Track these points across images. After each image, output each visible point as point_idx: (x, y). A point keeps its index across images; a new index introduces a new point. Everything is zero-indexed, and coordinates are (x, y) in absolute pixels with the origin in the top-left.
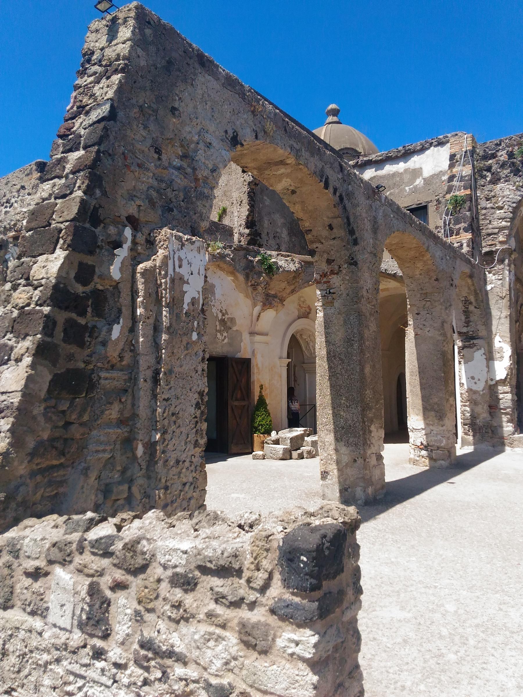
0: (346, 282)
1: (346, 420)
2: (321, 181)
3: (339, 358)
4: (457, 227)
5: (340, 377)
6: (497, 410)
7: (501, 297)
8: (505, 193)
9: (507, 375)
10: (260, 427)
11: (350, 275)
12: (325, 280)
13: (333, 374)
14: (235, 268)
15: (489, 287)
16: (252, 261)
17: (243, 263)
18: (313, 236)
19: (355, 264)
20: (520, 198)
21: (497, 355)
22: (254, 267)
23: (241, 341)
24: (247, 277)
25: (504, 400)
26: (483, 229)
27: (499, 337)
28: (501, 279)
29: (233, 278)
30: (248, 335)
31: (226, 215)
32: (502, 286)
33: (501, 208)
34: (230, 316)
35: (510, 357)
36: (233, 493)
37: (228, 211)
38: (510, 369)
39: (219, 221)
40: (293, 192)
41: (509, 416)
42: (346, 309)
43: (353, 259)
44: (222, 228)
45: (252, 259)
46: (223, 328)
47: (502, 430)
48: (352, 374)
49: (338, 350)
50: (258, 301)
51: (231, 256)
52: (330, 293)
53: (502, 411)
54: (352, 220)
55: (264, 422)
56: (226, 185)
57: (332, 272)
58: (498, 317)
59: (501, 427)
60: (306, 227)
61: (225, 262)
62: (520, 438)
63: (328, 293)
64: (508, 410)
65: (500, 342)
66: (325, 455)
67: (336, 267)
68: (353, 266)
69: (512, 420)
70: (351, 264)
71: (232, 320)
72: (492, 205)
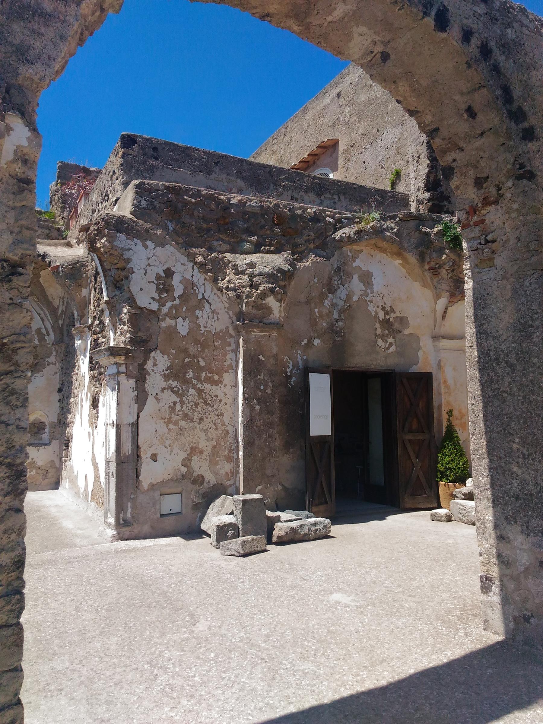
0: (514, 215)
1: (523, 483)
2: (426, 14)
3: (507, 362)
5: (509, 398)
10: (448, 472)
11: (520, 199)
12: (475, 218)
13: (496, 392)
14: (401, 246)
16: (428, 234)
17: (415, 238)
18: (444, 139)
19: (531, 176)
22: (431, 242)
23: (419, 348)
24: (422, 258)
29: (401, 262)
30: (431, 340)
31: (400, 180)
34: (398, 314)
36: (340, 590)
37: (402, 174)
39: (392, 188)
40: (385, 57)
42: (516, 267)
43: (522, 166)
44: (391, 198)
45: (429, 230)
46: (386, 332)
48: (532, 392)
49: (503, 347)
50: (443, 290)
51: (395, 230)
52: (487, 242)
54: (517, 92)
55: (453, 465)
56: (400, 139)
57: (487, 202)
60: (428, 125)
61: (385, 239)
63: (483, 242)
66: (487, 546)
67: (493, 190)
68: (524, 181)
70: (519, 178)
71: (403, 320)
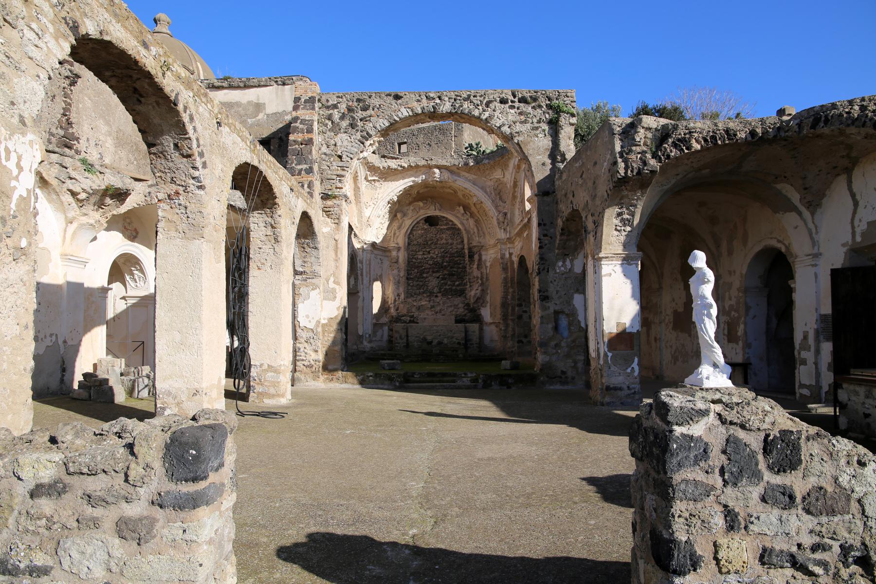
4: (299, 167)
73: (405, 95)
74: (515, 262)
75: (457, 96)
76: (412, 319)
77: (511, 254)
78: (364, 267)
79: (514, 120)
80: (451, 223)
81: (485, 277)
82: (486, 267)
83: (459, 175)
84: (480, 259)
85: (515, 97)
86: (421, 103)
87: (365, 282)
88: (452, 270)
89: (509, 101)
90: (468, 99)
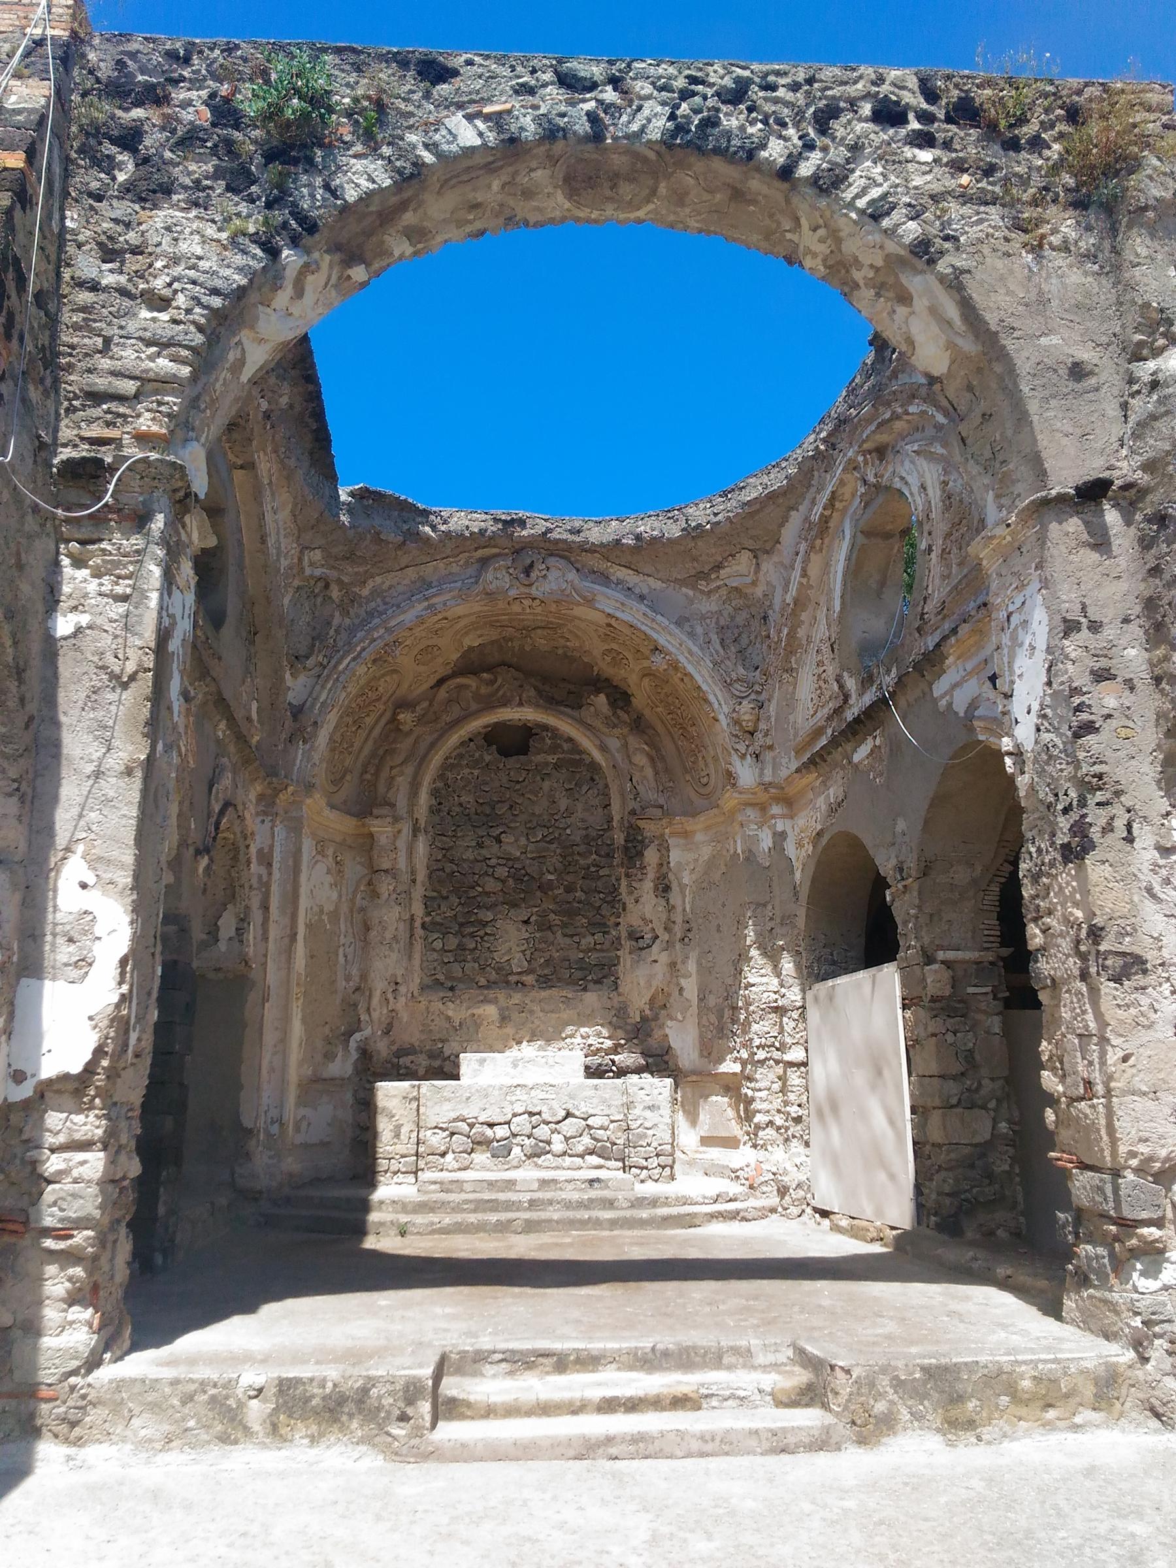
6: (27, 1241)
7: (113, 676)
8: (183, 247)
9: (99, 1052)
15: (64, 625)
20: (241, 280)
21: (64, 953)
25: (65, 1186)
26: (70, 368)
27: (84, 865)
28: (125, 598)
32: (126, 627)
33: (161, 303)
35: (123, 962)
38: (120, 1024)
41: (78, 1271)
47: (35, 1349)
53: (49, 1243)
58: (90, 768)
59: (32, 1328)
62: (120, 1385)
64: (81, 1237)
65: (84, 886)
69: (95, 1288)
72: (123, 279)
73: (470, 63)
74: (798, 865)
75: (693, 80)
76: (437, 1063)
77: (780, 837)
78: (276, 875)
79: (936, 187)
80: (566, 746)
81: (679, 919)
82: (682, 887)
83: (604, 579)
84: (664, 863)
85: (931, 96)
86: (535, 100)
87: (274, 932)
88: (570, 897)
89: (911, 116)
90: (736, 95)
